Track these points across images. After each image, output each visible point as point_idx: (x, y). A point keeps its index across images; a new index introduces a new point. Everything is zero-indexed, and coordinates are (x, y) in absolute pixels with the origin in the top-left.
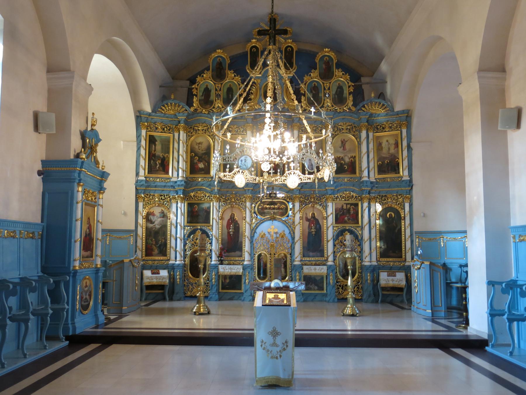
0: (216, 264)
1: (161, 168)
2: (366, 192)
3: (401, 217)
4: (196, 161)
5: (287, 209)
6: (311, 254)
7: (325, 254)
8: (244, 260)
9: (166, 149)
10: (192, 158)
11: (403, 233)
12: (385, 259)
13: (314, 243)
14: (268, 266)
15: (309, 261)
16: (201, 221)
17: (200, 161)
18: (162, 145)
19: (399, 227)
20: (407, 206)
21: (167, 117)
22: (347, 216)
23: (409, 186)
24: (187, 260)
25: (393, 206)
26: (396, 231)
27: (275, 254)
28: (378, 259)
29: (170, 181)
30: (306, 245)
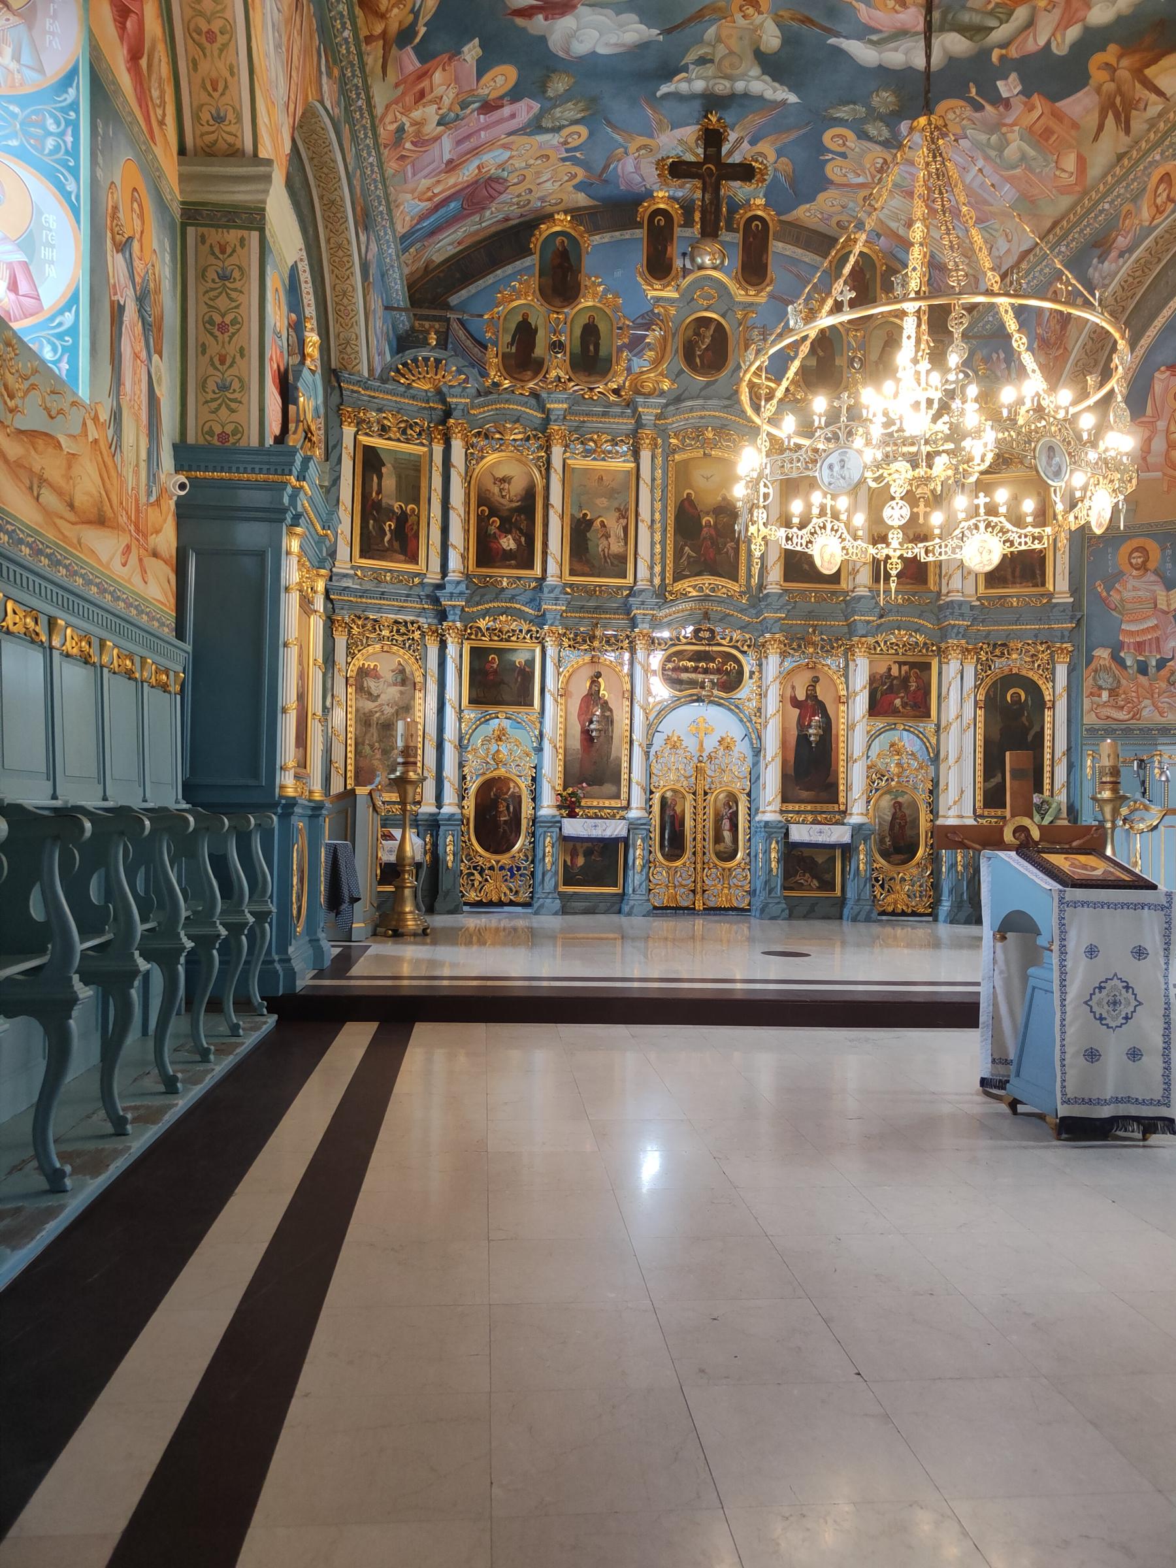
0: (554, 816)
1: (396, 545)
2: (958, 633)
3: (1044, 703)
4: (493, 529)
5: (741, 672)
6: (805, 794)
7: (841, 794)
8: (627, 807)
9: (411, 488)
10: (482, 521)
11: (1047, 744)
13: (812, 769)
14: (688, 823)
15: (798, 812)
16: (506, 697)
17: (505, 529)
18: (399, 478)
19: (1036, 728)
20: (1061, 671)
21: (413, 398)
22: (902, 696)
23: (1072, 618)
24: (470, 804)
25: (1024, 673)
26: (1030, 738)
27: (706, 794)
28: (979, 812)
29: (421, 583)
30: (791, 772)
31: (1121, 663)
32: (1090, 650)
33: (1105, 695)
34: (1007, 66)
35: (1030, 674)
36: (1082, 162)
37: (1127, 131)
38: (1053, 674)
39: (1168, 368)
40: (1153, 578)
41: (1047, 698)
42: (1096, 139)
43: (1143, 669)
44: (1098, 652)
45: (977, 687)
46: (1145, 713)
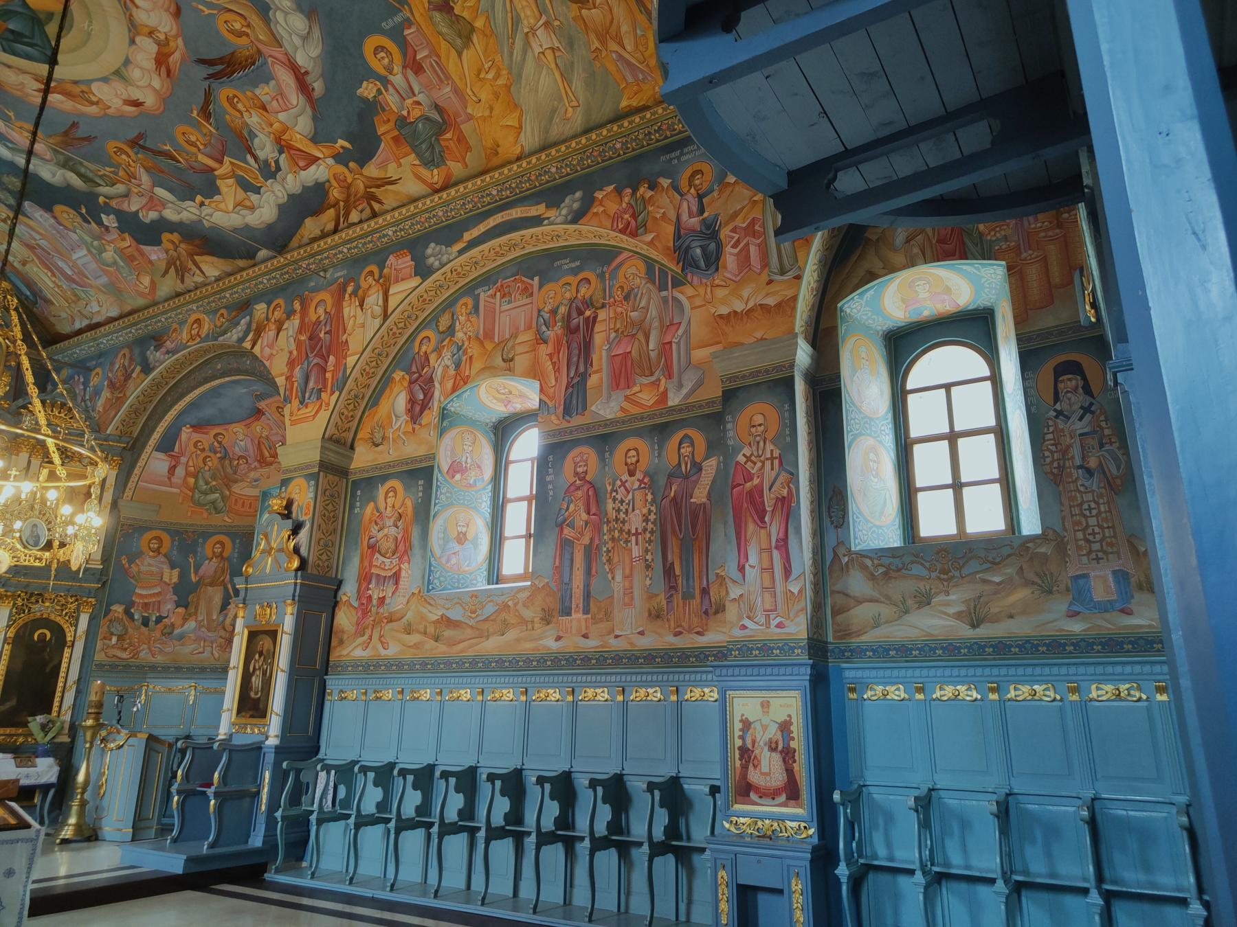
3: (66, 642)
11: (62, 674)
12: (8, 731)
19: (55, 662)
20: (84, 620)
23: (98, 581)
25: (52, 617)
26: (48, 670)
31: (131, 617)
32: (109, 605)
33: (114, 639)
34: (107, 209)
35: (58, 619)
36: (153, 284)
37: (182, 282)
38: (77, 620)
39: (192, 426)
40: (163, 559)
41: (69, 639)
42: (163, 276)
43: (145, 622)
44: (113, 608)
45: (9, 626)
46: (142, 654)
